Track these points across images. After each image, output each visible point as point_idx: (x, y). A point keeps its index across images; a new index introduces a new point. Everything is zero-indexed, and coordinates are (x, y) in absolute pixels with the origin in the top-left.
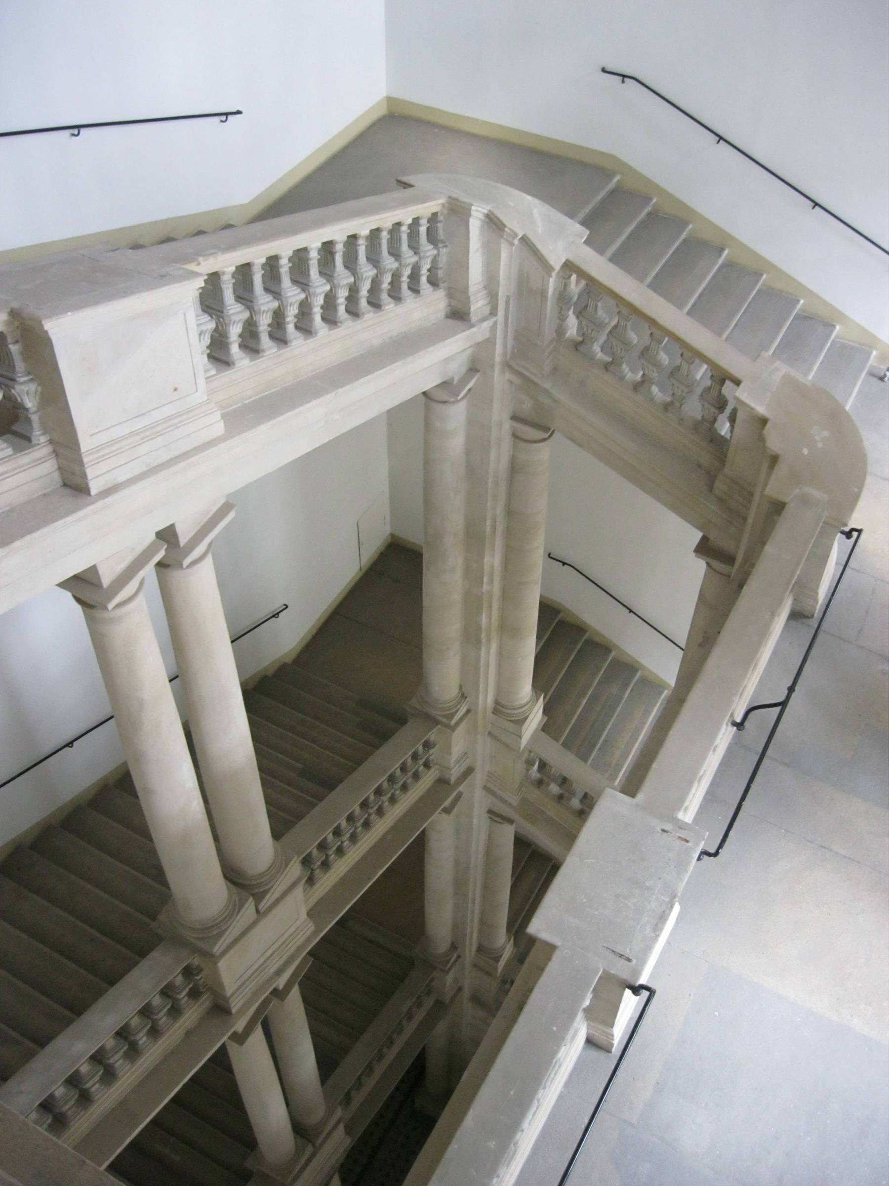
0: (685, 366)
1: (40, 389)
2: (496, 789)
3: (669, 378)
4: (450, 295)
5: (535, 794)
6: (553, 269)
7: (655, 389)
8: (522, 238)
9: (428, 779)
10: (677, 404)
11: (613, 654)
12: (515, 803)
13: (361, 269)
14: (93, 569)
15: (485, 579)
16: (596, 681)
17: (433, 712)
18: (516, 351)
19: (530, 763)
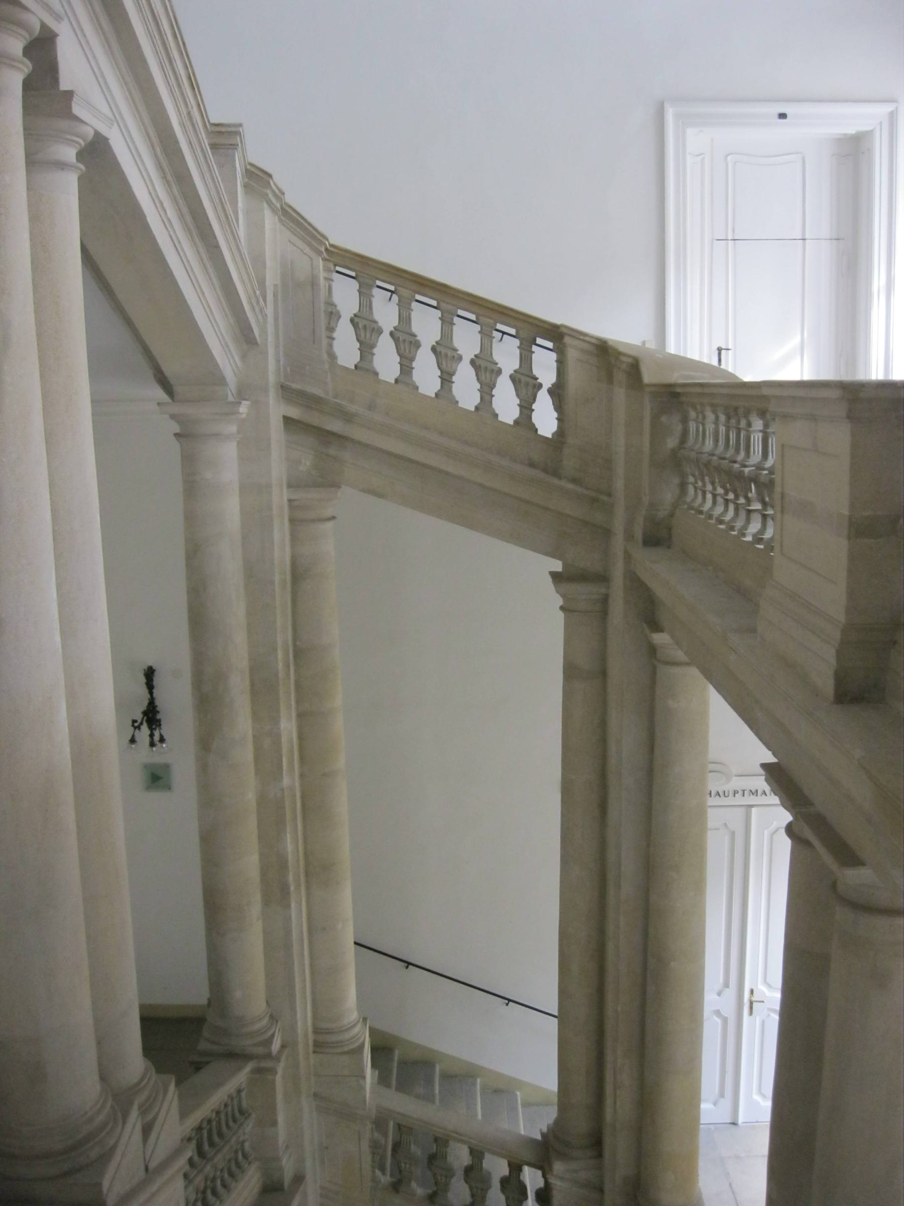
11: (396, 1054)
18: (289, 369)
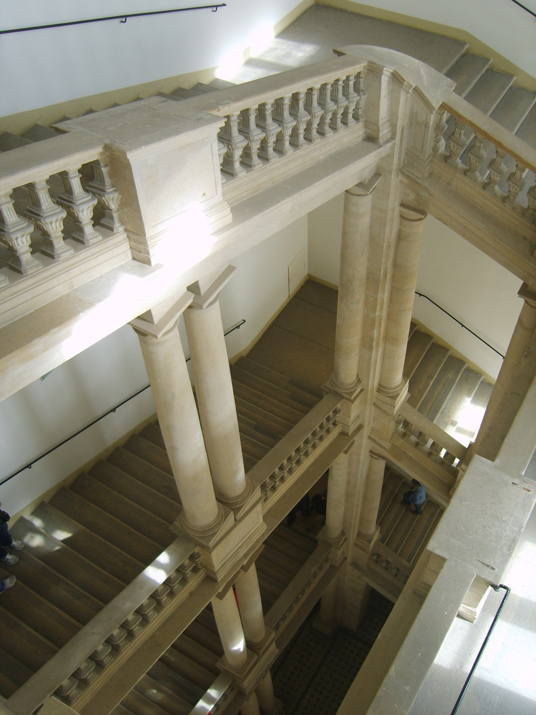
0: (518, 173)
1: (120, 196)
2: (376, 439)
3: (507, 181)
4: (366, 126)
5: (400, 442)
6: (435, 109)
7: (497, 188)
8: (414, 88)
9: (335, 433)
10: (512, 198)
12: (388, 447)
13: (314, 110)
14: (149, 313)
15: (378, 308)
16: (439, 370)
17: (339, 391)
19: (398, 423)
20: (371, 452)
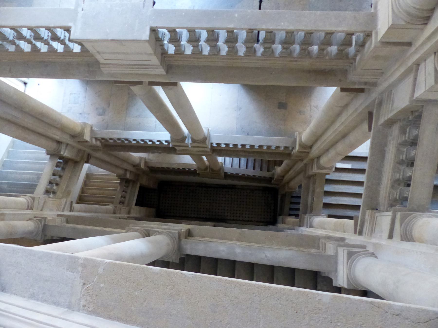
2: (63, 207)
12: (65, 200)
20: (70, 211)
